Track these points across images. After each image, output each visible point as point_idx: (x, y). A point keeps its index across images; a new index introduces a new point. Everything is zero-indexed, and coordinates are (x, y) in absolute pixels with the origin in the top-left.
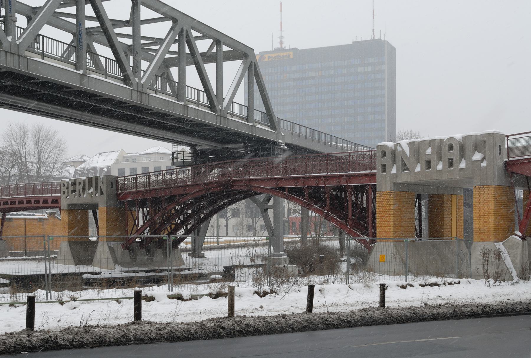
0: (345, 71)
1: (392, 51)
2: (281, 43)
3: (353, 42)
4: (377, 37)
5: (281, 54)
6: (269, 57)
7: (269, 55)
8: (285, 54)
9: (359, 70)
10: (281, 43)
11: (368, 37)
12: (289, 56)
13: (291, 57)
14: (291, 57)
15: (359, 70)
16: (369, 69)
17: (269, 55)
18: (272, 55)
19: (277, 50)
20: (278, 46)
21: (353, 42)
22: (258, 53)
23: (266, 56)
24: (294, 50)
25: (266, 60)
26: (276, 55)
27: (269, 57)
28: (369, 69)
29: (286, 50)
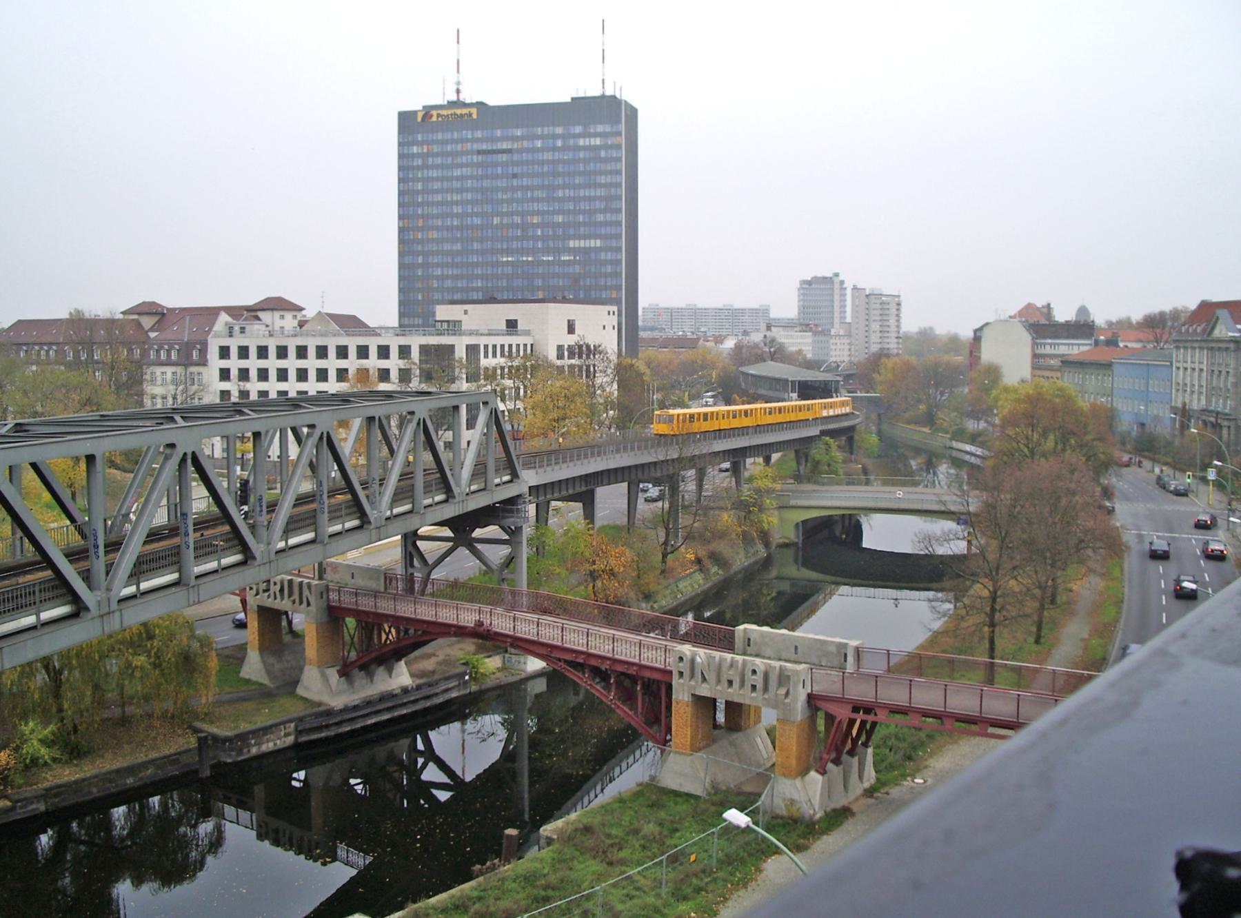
0: (559, 143)
1: (633, 113)
2: (458, 92)
3: (572, 99)
4: (609, 92)
5: (459, 112)
6: (438, 115)
7: (440, 112)
8: (465, 111)
9: (581, 142)
10: (458, 92)
11: (595, 91)
12: (470, 115)
13: (475, 116)
14: (475, 116)
15: (581, 142)
16: (598, 141)
17: (440, 112)
18: (445, 112)
19: (452, 104)
20: (454, 98)
21: (572, 99)
22: (421, 108)
23: (434, 113)
24: (480, 105)
25: (434, 119)
26: (449, 112)
27: (438, 115)
28: (598, 141)
29: (465, 105)
